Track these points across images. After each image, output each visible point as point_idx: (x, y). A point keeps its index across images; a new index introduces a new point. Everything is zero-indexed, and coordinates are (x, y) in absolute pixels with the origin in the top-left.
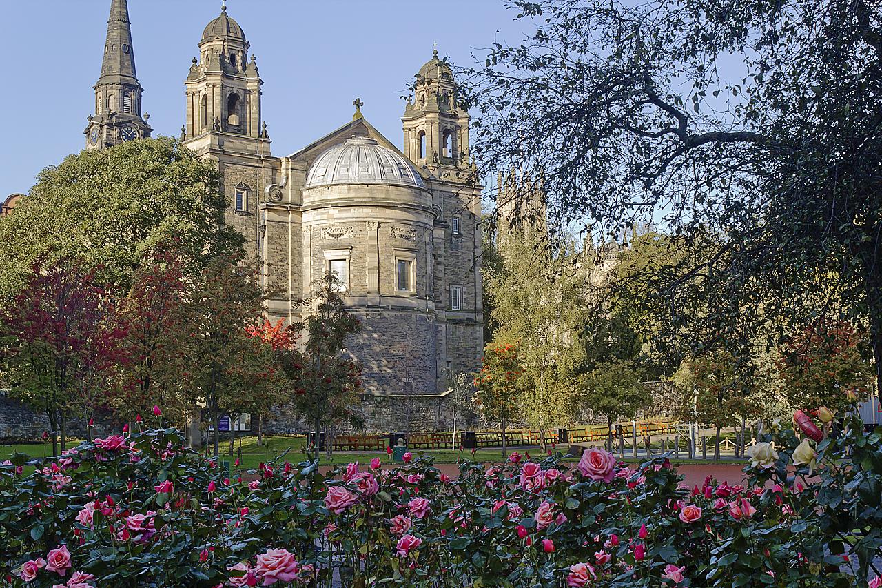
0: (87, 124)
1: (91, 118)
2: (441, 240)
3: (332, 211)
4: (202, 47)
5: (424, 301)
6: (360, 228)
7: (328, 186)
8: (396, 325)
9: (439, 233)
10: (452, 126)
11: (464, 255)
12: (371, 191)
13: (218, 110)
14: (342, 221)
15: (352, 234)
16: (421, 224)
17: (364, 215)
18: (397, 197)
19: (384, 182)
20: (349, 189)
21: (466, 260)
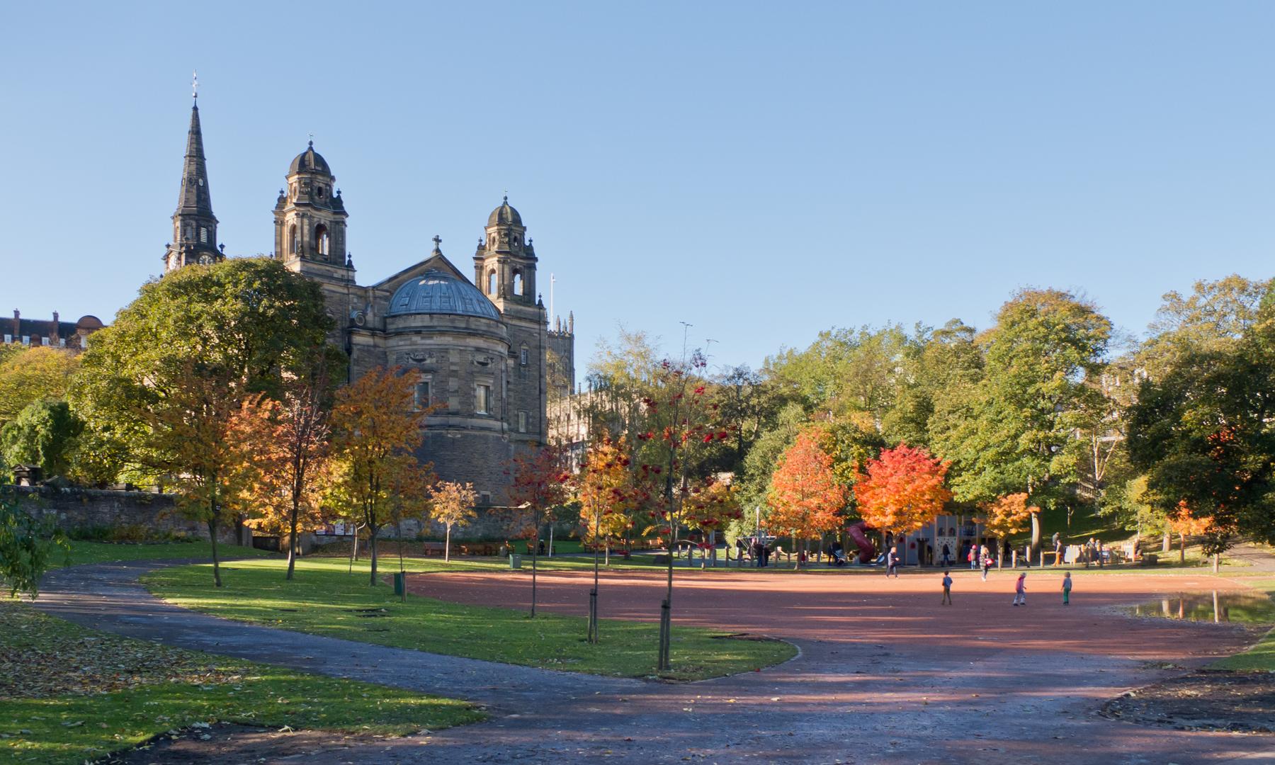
0: (165, 251)
1: (168, 246)
3: (417, 339)
4: (290, 179)
5: (499, 423)
6: (442, 354)
7: (411, 314)
9: (511, 362)
11: (530, 383)
12: (453, 321)
13: (306, 239)
14: (424, 347)
15: (434, 360)
17: (446, 343)
18: (477, 328)
19: (464, 314)
20: (432, 319)
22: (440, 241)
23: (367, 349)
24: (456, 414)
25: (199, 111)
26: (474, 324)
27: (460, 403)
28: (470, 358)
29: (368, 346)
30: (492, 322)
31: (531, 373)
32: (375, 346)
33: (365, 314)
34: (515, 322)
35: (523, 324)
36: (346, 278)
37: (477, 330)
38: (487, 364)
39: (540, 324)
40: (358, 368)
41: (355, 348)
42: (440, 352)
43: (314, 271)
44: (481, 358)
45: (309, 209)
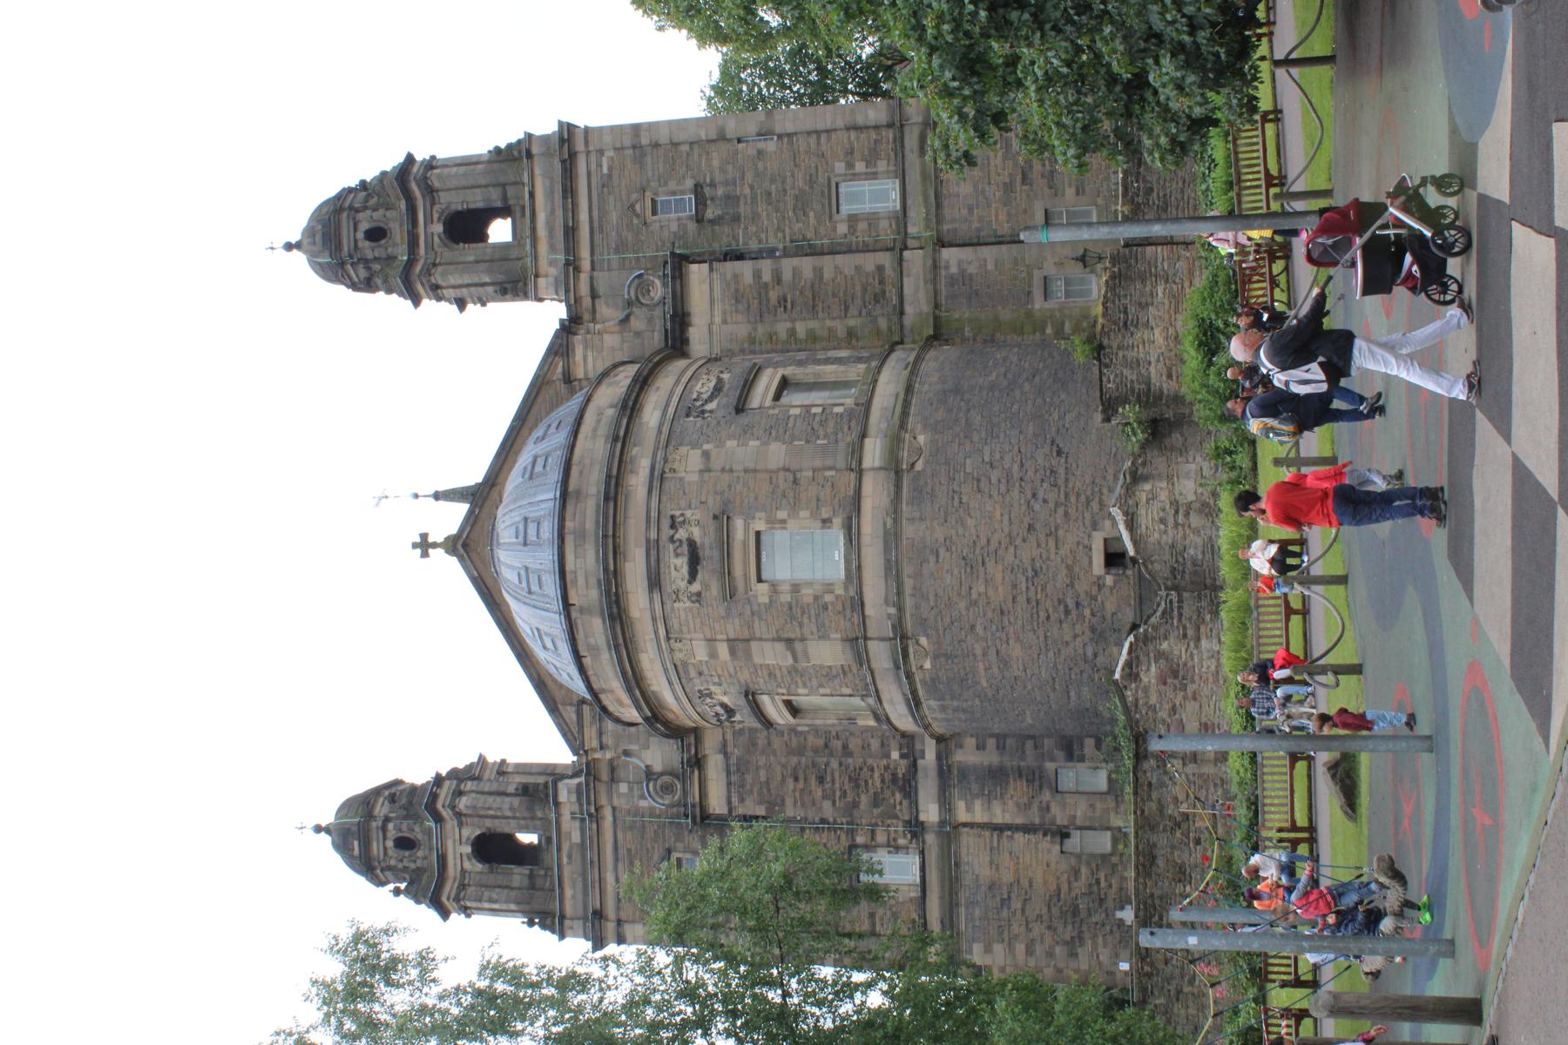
2: (715, 275)
6: (693, 673)
8: (941, 594)
10: (436, 216)
11: (749, 177)
17: (658, 667)
18: (593, 581)
21: (760, 165)
22: (424, 536)
23: (737, 772)
24: (857, 643)
25: (441, 489)
26: (587, 593)
27: (823, 637)
28: (684, 605)
29: (728, 773)
30: (569, 524)
31: (718, 177)
32: (724, 750)
33: (649, 774)
35: (584, 216)
36: (576, 808)
37: (599, 582)
38: (692, 544)
39: (573, 155)
40: (789, 802)
41: (741, 811)
43: (580, 897)
44: (677, 566)
45: (444, 899)
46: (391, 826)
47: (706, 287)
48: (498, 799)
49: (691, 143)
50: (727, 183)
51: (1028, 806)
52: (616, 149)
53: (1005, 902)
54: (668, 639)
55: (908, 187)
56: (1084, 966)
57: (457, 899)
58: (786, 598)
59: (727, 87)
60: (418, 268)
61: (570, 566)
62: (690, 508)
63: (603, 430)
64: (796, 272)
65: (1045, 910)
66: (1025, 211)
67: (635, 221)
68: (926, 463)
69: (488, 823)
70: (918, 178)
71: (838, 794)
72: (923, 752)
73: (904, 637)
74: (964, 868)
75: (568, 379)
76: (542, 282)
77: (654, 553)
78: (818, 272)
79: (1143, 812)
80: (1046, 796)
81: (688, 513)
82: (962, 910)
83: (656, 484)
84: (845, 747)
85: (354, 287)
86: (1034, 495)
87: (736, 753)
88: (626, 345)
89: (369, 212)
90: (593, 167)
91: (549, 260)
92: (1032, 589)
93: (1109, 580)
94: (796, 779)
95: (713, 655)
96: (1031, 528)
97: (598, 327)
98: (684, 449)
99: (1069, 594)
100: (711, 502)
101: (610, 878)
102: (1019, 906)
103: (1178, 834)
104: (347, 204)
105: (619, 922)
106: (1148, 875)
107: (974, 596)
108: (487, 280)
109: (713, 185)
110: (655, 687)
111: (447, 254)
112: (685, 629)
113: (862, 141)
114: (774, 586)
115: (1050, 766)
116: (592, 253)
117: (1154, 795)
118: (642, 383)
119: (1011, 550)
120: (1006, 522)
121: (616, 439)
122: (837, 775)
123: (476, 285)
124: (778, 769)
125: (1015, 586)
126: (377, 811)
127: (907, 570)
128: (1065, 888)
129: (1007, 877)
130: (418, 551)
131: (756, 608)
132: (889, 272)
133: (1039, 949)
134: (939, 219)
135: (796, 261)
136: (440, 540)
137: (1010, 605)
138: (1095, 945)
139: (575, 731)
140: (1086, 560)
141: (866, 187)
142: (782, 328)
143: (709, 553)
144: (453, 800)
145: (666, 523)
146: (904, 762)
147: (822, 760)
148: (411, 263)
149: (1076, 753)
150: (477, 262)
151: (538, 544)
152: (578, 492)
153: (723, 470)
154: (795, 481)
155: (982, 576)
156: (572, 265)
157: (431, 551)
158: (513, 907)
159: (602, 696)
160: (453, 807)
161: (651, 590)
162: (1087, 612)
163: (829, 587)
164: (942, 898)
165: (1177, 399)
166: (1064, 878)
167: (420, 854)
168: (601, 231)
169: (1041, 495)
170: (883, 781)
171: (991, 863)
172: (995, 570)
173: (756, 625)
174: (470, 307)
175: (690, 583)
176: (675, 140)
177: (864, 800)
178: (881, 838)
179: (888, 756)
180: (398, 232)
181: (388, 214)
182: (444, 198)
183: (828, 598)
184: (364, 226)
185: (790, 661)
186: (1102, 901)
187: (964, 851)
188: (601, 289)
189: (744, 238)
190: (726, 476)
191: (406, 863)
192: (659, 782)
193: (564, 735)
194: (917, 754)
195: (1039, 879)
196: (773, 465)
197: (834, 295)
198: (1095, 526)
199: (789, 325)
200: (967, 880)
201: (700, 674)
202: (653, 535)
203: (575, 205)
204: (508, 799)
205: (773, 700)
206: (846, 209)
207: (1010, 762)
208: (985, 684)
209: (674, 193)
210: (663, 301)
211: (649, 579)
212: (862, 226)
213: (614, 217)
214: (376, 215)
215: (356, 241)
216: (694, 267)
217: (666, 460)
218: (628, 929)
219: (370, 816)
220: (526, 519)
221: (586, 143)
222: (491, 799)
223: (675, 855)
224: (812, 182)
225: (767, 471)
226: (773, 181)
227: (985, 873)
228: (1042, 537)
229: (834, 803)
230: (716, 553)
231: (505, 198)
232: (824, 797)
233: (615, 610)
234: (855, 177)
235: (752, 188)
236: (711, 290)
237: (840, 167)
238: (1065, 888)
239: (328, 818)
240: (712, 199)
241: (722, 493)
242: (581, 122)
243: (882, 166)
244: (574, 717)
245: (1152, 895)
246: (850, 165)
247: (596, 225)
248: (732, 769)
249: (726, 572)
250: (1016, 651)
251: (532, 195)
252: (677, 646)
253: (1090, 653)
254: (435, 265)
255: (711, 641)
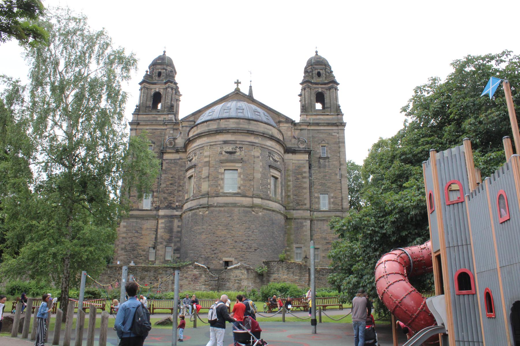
2: (305, 161)
6: (201, 151)
8: (220, 217)
10: (323, 90)
11: (330, 171)
16: (247, 143)
18: (226, 126)
22: (240, 83)
23: (174, 162)
24: (207, 195)
25: (252, 88)
26: (223, 124)
27: (209, 186)
29: (174, 160)
30: (242, 121)
31: (331, 163)
32: (180, 159)
33: (175, 139)
34: (312, 128)
35: (322, 128)
36: (167, 119)
38: (235, 152)
39: (337, 126)
40: (166, 175)
41: (164, 163)
42: (199, 151)
43: (143, 119)
44: (229, 148)
45: (144, 84)
46: (164, 71)
47: (302, 159)
48: (170, 99)
49: (339, 157)
50: (329, 165)
51: (162, 238)
52: (339, 137)
53: (137, 232)
54: (210, 145)
55: (326, 212)
56: (119, 252)
57: (144, 87)
58: (220, 177)
59: (354, 167)
60: (310, 85)
61: (231, 120)
62: (245, 152)
63: (266, 131)
64: (305, 182)
65: (134, 242)
66: (319, 243)
67: (320, 141)
68: (254, 215)
69: (164, 96)
70: (329, 215)
71: (168, 188)
72: (178, 211)
73: (208, 207)
74: (146, 221)
75: (280, 122)
76: (305, 116)
77: (233, 142)
78: (305, 188)
79: (159, 269)
80: (165, 244)
81: (243, 152)
82: (135, 220)
83: (251, 144)
84: (180, 191)
85: (306, 68)
86: (244, 243)
87: (179, 162)
88: (288, 137)
89: (325, 73)
90: (334, 131)
91: (311, 118)
92: (220, 242)
93: (221, 262)
94: (172, 178)
95: (206, 157)
96: (236, 242)
97: (293, 130)
98: (260, 151)
99: (218, 251)
100: (246, 158)
101: (148, 127)
102: (136, 235)
103: (153, 278)
104: (327, 67)
105: (136, 129)
106: (143, 270)
107: (219, 226)
108: (306, 102)
109: (329, 162)
110: (198, 141)
111: (313, 92)
112: (213, 150)
113: (338, 201)
114: (223, 174)
115: (173, 245)
116: (312, 130)
117: (164, 272)
118: (278, 141)
119: (230, 236)
120: (238, 235)
121: (263, 134)
122: (172, 188)
123: (305, 99)
124: (175, 173)
125: (221, 237)
126: (168, 67)
127: (226, 209)
128: (140, 248)
129: (143, 232)
130: (236, 81)
131: (217, 168)
132: (304, 207)
133: (124, 240)
134: (318, 220)
135: (308, 183)
136: (239, 87)
137: (217, 235)
138: (124, 255)
139: (187, 120)
140: (227, 256)
141: (327, 202)
142: (291, 178)
143: (232, 157)
144: (170, 87)
145: (241, 146)
146: (175, 206)
147: (177, 184)
148: (311, 83)
149: (176, 252)
150: (311, 100)
151: (237, 112)
152: (250, 123)
153: (254, 161)
154: (250, 180)
155: (224, 228)
156: (309, 124)
157: (236, 84)
158: (141, 102)
159: (196, 127)
160: (169, 87)
161: (223, 141)
162: (213, 256)
163: (222, 188)
164: (139, 215)
165: (268, 281)
166: (142, 247)
167: (157, 78)
168: (319, 132)
169: (245, 245)
170: (170, 200)
171: (148, 228)
172: (225, 232)
173: (213, 168)
174: (299, 97)
175: (225, 151)
176: (340, 153)
177: (166, 195)
178: (155, 199)
179: (177, 202)
180: (319, 80)
181: (324, 78)
182: (328, 92)
183: (219, 188)
184: (321, 71)
185: (203, 177)
186: (136, 257)
187: (151, 221)
188: (302, 131)
189: (314, 170)
190: (253, 162)
191: (154, 74)
192: (173, 141)
193: (186, 117)
194: (177, 210)
195: (142, 241)
196: (255, 174)
197: (299, 192)
198: (236, 259)
199: (292, 180)
200: (143, 222)
201: (201, 153)
202: (238, 142)
203: (324, 126)
204: (170, 101)
205: (193, 172)
206: (321, 196)
207: (174, 234)
208: (195, 228)
209: (327, 151)
210: (299, 147)
211: (226, 141)
212: (317, 200)
213: (321, 136)
214: (324, 75)
215: (317, 69)
216: (307, 156)
217: (257, 146)
218: (134, 132)
219: (167, 65)
220: (243, 109)
221: (340, 129)
222: (170, 97)
223: (153, 145)
224: (328, 187)
225: (254, 173)
226: (329, 177)
227: (145, 227)
228: (233, 245)
229: (165, 187)
230: (232, 159)
231: (327, 108)
232: (167, 185)
233: (218, 132)
234: (329, 199)
235: (328, 172)
236: (301, 160)
237: (332, 195)
238: (140, 248)
239: (167, 55)
240: (325, 161)
241: (248, 161)
242: (346, 128)
243: (332, 206)
244: (191, 120)
245: (137, 271)
246: (332, 197)
247: (319, 131)
248: (175, 161)
249: (227, 161)
250: (204, 236)
251: (328, 115)
252: (209, 148)
253: (203, 256)
254: (311, 89)
255: (209, 157)
